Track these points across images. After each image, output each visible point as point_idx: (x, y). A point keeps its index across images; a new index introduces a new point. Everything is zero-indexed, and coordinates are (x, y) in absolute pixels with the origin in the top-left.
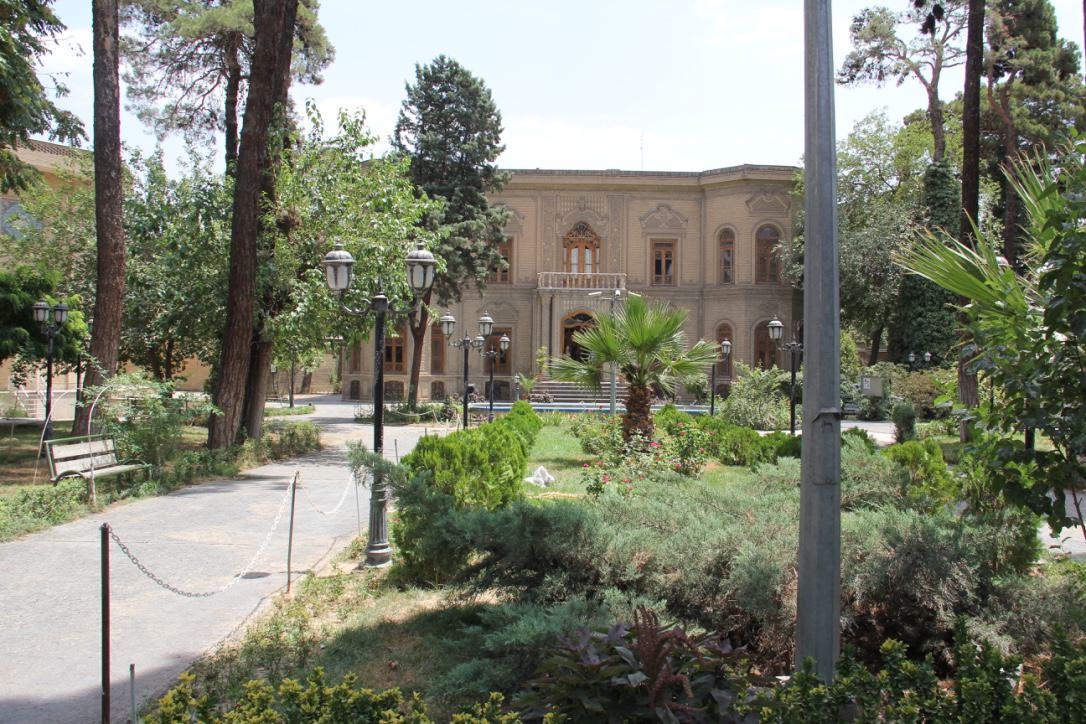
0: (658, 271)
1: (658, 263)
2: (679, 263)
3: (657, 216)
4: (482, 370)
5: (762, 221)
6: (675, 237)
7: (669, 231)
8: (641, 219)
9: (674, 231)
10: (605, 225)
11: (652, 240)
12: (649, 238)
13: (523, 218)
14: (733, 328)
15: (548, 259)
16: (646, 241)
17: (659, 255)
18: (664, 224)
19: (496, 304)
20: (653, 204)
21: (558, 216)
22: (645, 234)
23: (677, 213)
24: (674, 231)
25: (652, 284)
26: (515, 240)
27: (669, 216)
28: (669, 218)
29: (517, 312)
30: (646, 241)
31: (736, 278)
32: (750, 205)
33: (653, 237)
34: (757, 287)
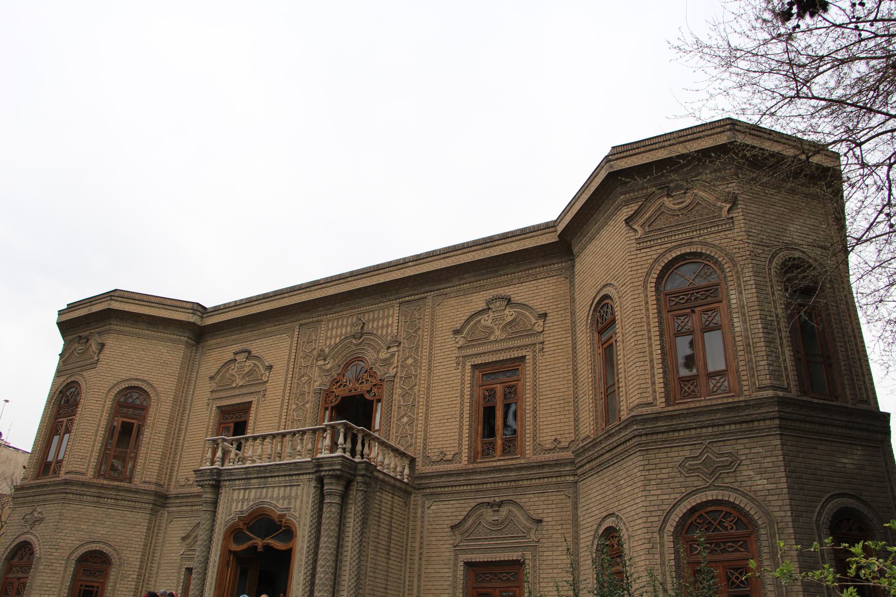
0: (489, 431)
1: (489, 413)
2: (529, 407)
3: (487, 320)
5: (670, 250)
6: (519, 354)
7: (510, 344)
8: (456, 332)
9: (527, 341)
10: (393, 355)
13: (270, 368)
17: (492, 393)
18: (497, 333)
20: (478, 301)
21: (322, 356)
22: (461, 361)
23: (523, 305)
24: (517, 343)
25: (473, 459)
26: (254, 406)
27: (509, 314)
33: (479, 361)
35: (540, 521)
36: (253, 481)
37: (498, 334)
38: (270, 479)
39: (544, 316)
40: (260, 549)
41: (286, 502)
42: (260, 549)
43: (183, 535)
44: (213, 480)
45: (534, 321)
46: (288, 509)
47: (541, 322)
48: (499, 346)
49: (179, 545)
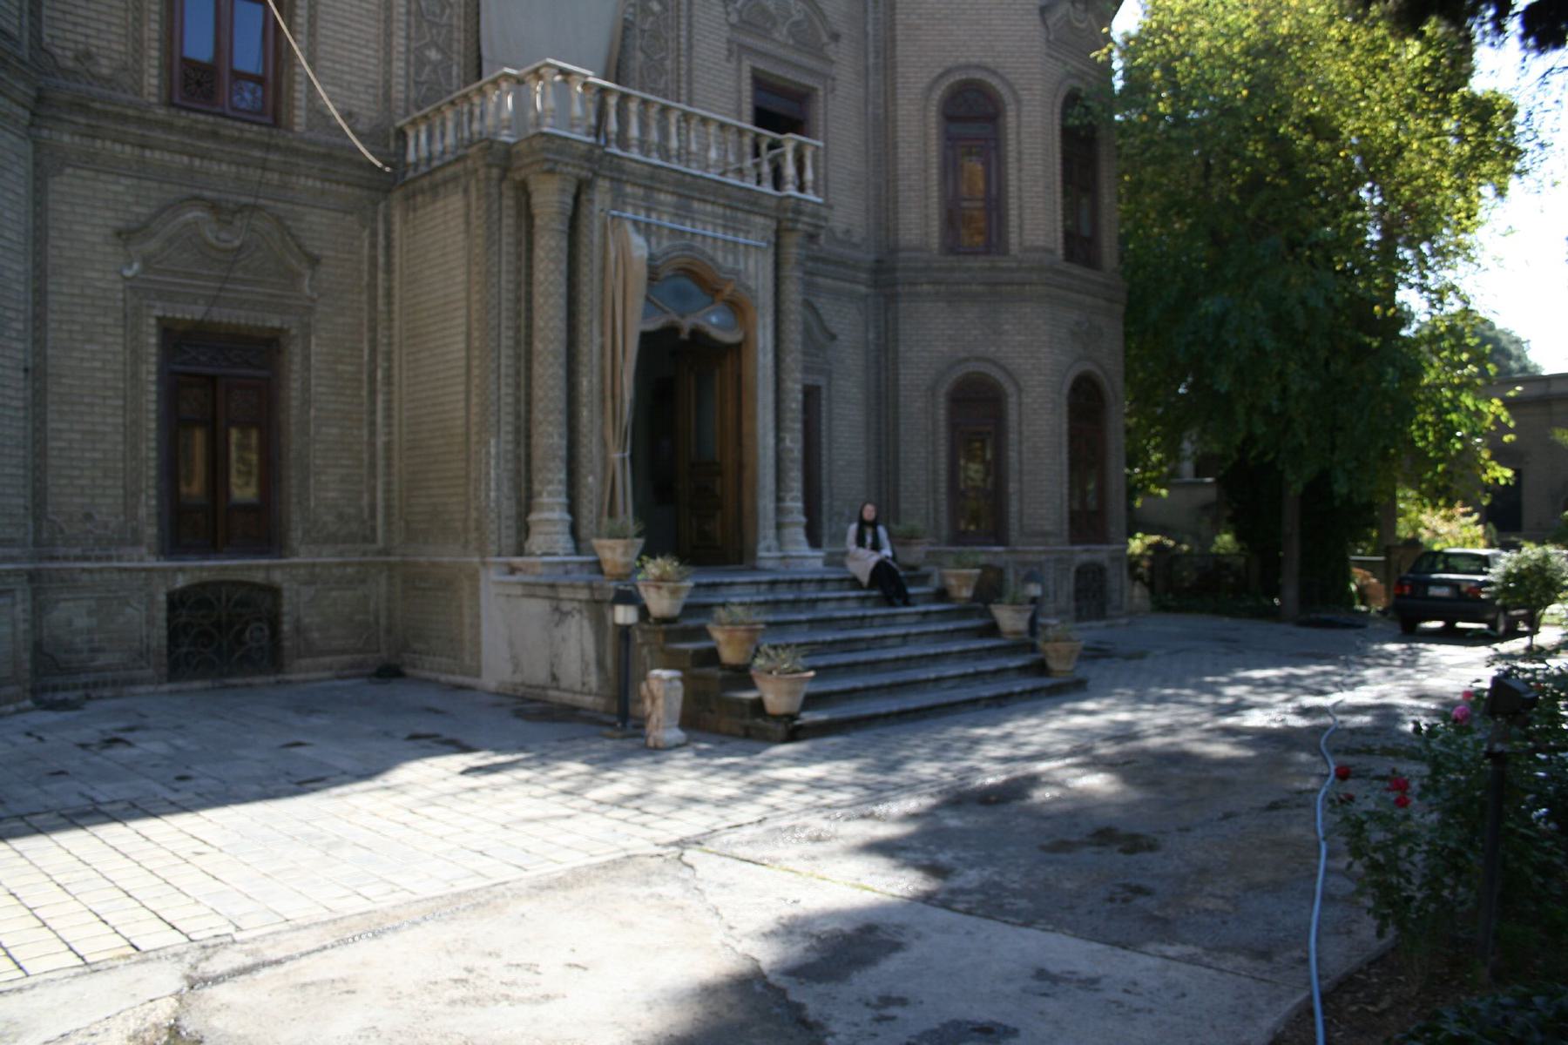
4: (151, 531)
6: (808, 81)
7: (795, 57)
11: (754, 70)
12: (746, 65)
14: (1010, 388)
15: (433, 55)
16: (739, 70)
18: (781, 33)
19: (214, 207)
22: (737, 50)
28: (797, 17)
29: (314, 261)
30: (739, 70)
31: (1014, 238)
32: (1051, 20)
34: (1064, 266)
35: (833, 337)
36: (662, 197)
37: (781, 33)
38: (696, 205)
39: (835, 37)
40: (684, 336)
41: (730, 258)
42: (684, 336)
43: (120, 224)
44: (590, 170)
45: (825, 39)
46: (737, 273)
47: (832, 46)
48: (781, 52)
49: (109, 249)
